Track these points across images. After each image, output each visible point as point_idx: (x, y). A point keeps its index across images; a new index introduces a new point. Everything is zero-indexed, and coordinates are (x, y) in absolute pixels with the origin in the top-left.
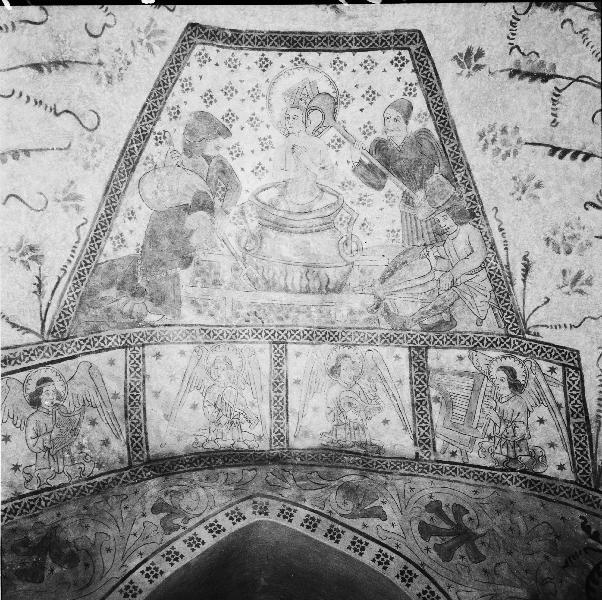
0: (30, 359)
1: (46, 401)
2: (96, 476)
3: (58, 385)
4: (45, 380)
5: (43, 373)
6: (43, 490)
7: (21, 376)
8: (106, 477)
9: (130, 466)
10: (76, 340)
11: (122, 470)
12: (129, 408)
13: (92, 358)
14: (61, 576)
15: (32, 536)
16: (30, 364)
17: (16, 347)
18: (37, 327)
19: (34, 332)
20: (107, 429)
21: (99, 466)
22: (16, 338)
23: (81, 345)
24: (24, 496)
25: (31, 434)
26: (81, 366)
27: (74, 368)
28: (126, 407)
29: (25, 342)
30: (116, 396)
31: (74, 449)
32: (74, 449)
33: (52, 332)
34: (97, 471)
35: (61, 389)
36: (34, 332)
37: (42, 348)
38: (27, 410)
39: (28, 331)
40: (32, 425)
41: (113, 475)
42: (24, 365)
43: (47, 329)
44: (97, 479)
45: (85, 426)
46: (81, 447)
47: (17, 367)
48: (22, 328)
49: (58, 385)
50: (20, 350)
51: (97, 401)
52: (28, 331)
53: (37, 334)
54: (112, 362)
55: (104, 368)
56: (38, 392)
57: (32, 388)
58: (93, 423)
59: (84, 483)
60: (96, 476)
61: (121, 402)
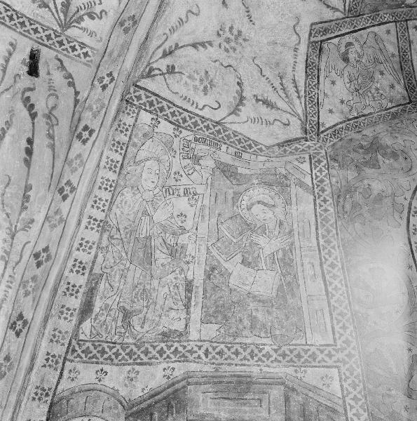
0: (340, 30)
1: (352, 56)
2: (390, 108)
3: (357, 47)
4: (349, 44)
5: (348, 39)
6: (360, 117)
7: (336, 41)
8: (396, 109)
9: (411, 102)
10: (365, 16)
11: (405, 104)
12: (402, 64)
13: (376, 29)
14: (391, 165)
15: (365, 143)
16: (340, 33)
17: (331, 21)
18: (341, 8)
19: (340, 11)
20: (391, 78)
21: (391, 101)
22: (328, 15)
23: (368, 20)
24: (351, 120)
25: (347, 80)
26: (370, 35)
27: (365, 36)
28: (401, 63)
29: (335, 18)
30: (393, 55)
31: (373, 91)
32: (373, 91)
33: (350, 11)
34: (390, 105)
35: (359, 50)
36: (340, 11)
37: (346, 22)
38: (341, 64)
39: (337, 10)
40: (346, 74)
41: (401, 107)
42: (336, 34)
43: (347, 8)
44: (391, 110)
45: (378, 76)
46: (377, 89)
47: (333, 35)
48: (333, 8)
49: (357, 47)
50: (334, 23)
51: (382, 58)
52: (337, 10)
53: (342, 12)
54: (388, 32)
55: (385, 37)
56: (347, 53)
57: (343, 49)
58: (382, 73)
59: (383, 113)
60: (390, 108)
61: (397, 59)
